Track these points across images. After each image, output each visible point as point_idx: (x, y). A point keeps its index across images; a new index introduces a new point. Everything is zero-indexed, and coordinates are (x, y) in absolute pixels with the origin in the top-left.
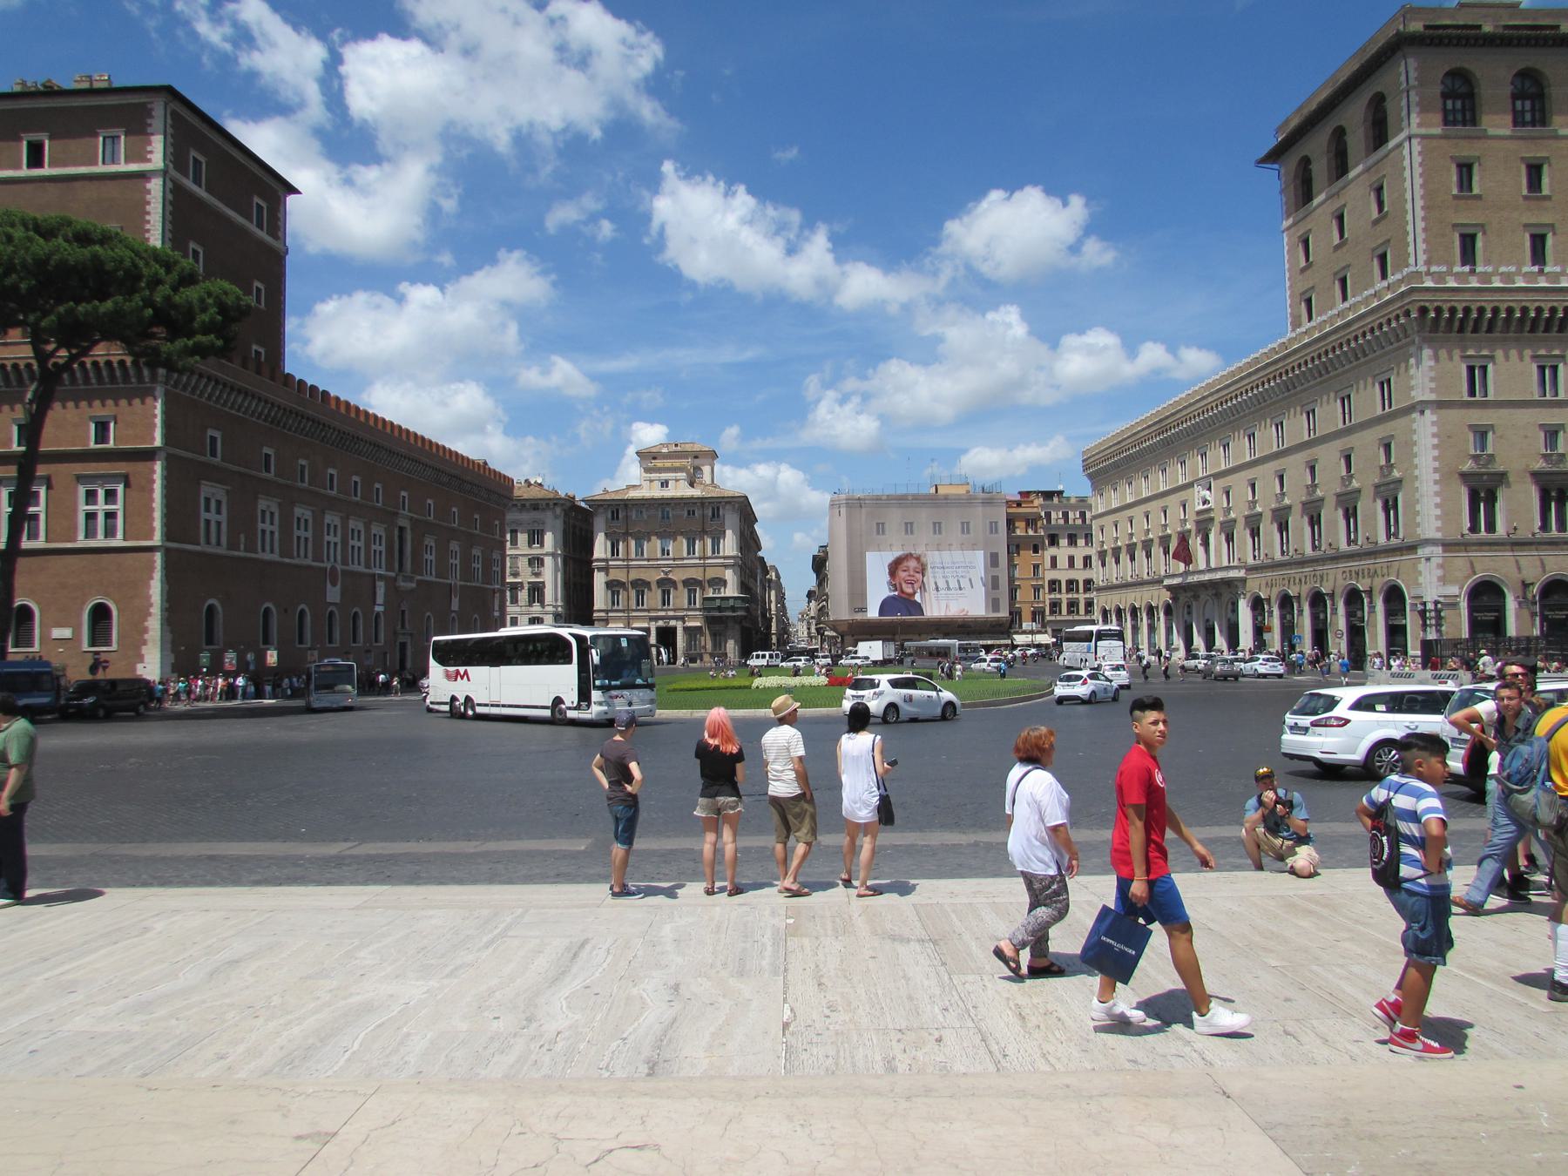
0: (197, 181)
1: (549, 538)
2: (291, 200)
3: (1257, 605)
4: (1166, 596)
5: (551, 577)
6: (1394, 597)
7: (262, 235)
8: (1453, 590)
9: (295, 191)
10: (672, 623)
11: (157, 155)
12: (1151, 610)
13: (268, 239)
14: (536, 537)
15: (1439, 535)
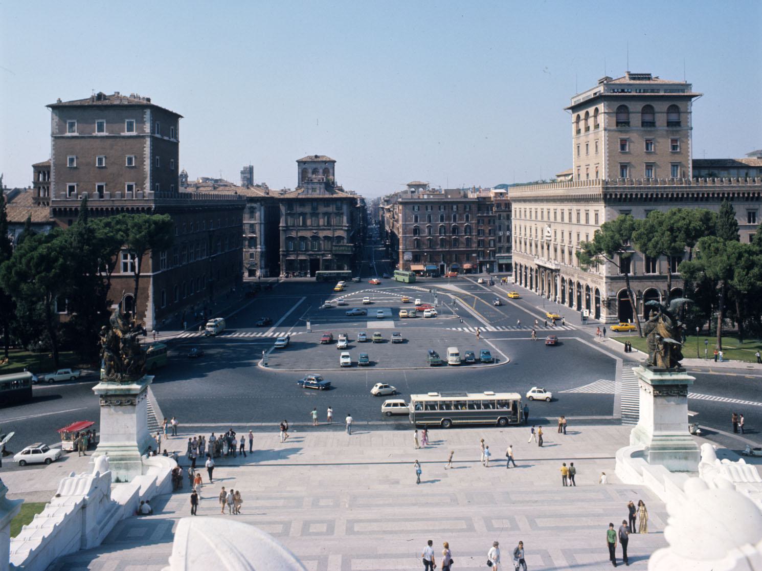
0: (158, 133)
1: (257, 214)
2: (181, 121)
3: (563, 280)
4: (537, 266)
5: (259, 234)
6: (597, 291)
7: (172, 140)
8: (614, 294)
9: (182, 117)
10: (318, 257)
11: (147, 128)
12: (531, 270)
13: (175, 141)
14: (252, 216)
15: (609, 275)
